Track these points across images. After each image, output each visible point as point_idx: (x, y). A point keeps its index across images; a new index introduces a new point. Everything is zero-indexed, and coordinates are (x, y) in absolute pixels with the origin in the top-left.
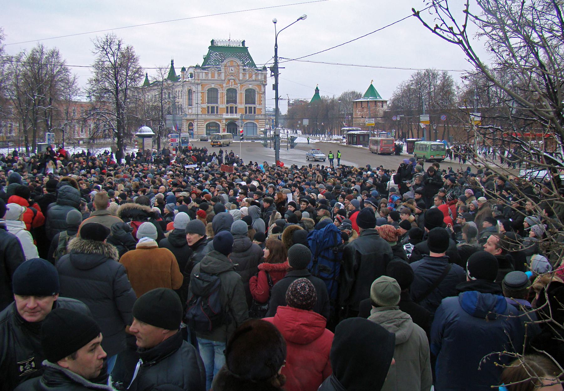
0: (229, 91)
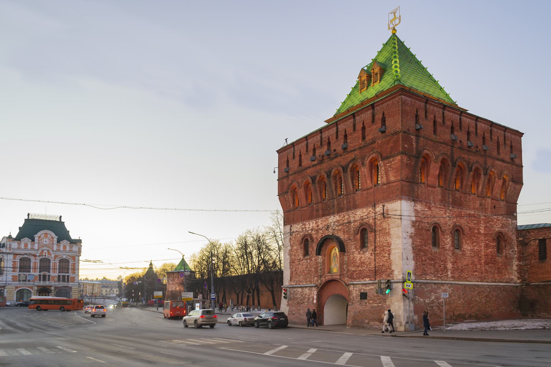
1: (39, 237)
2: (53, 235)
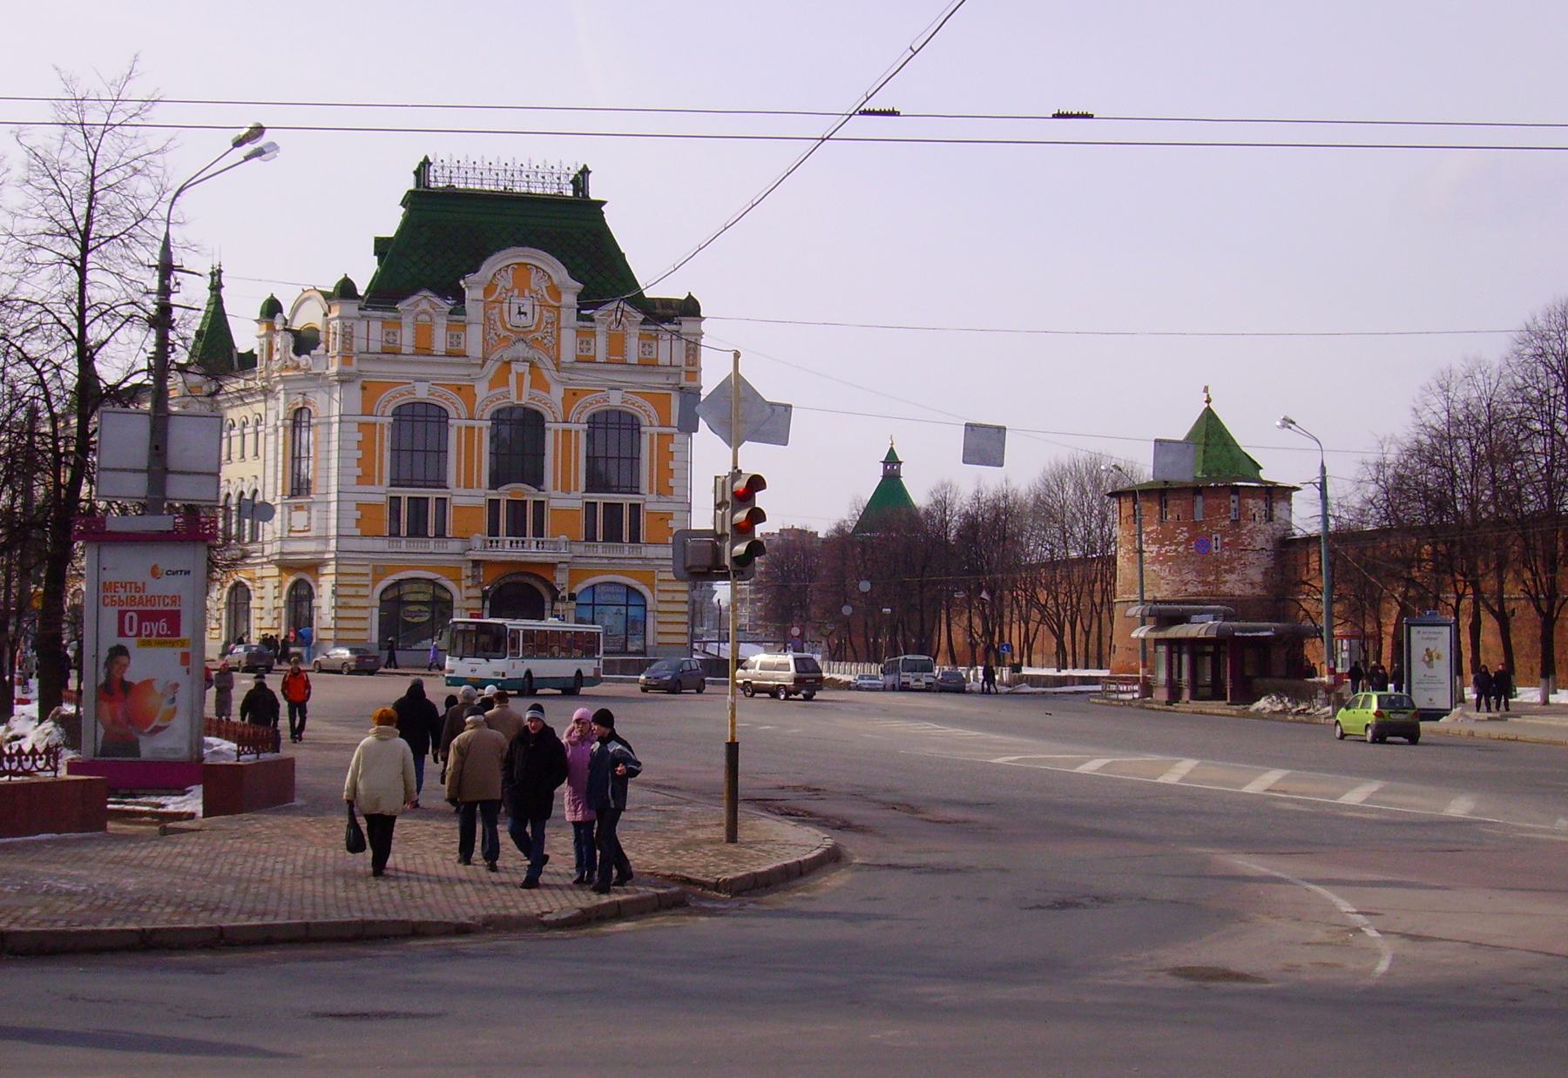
0: (498, 418)
1: (489, 289)
2: (560, 273)
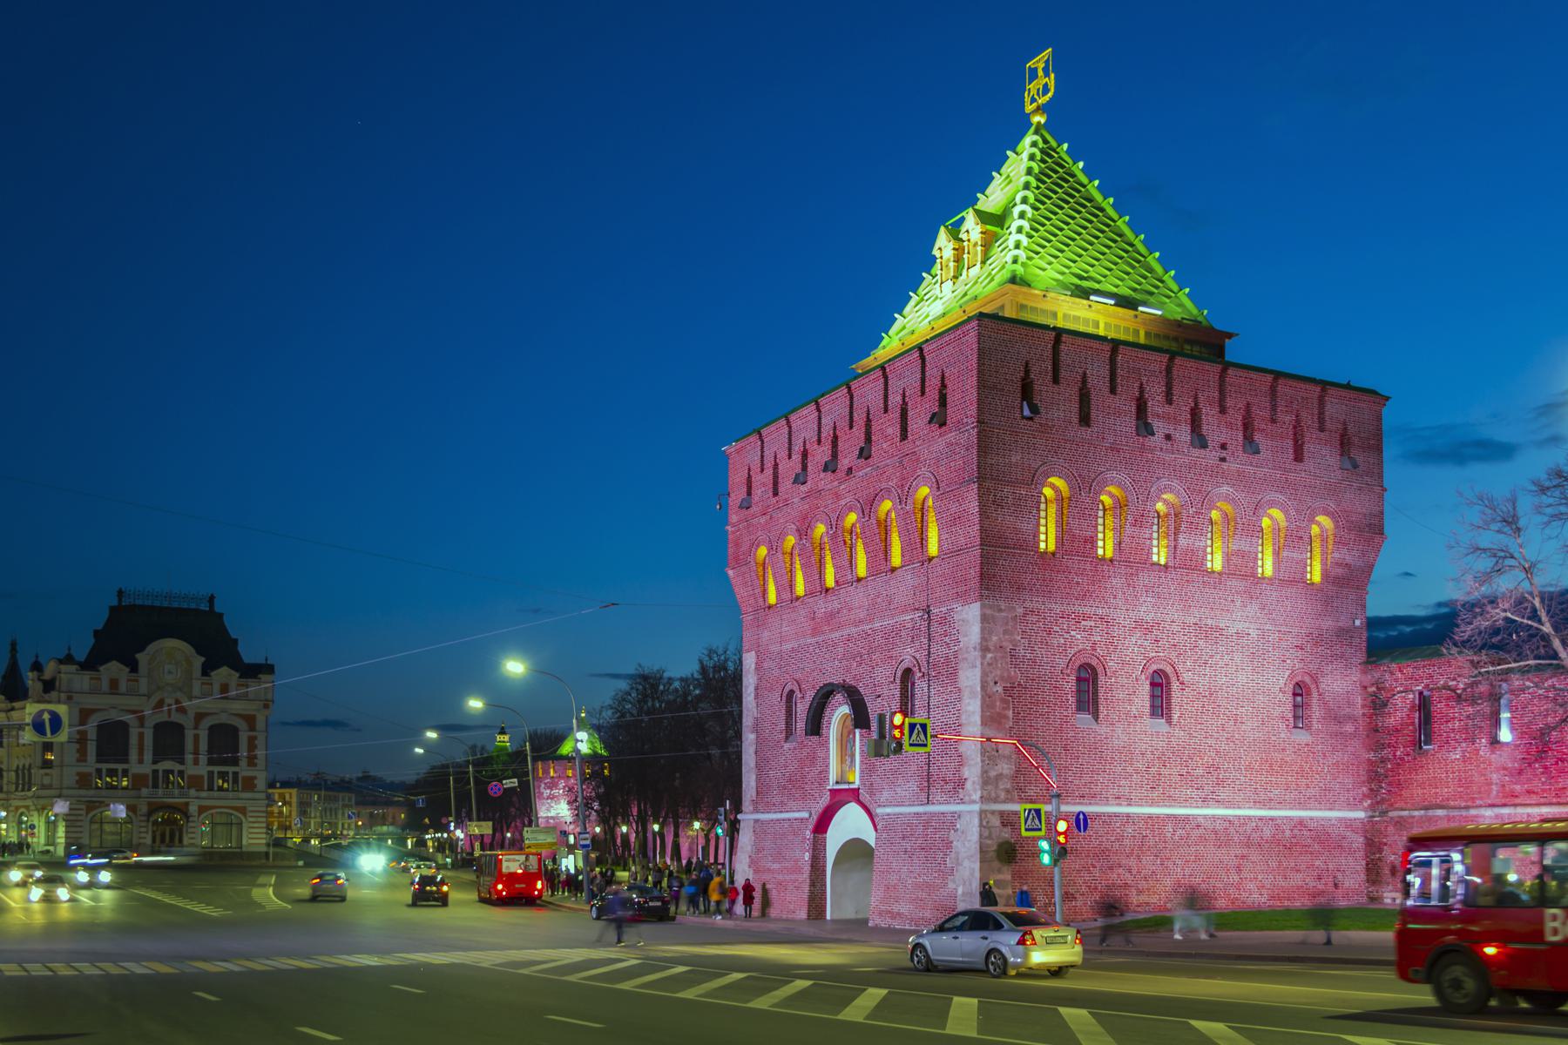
0: (160, 728)
